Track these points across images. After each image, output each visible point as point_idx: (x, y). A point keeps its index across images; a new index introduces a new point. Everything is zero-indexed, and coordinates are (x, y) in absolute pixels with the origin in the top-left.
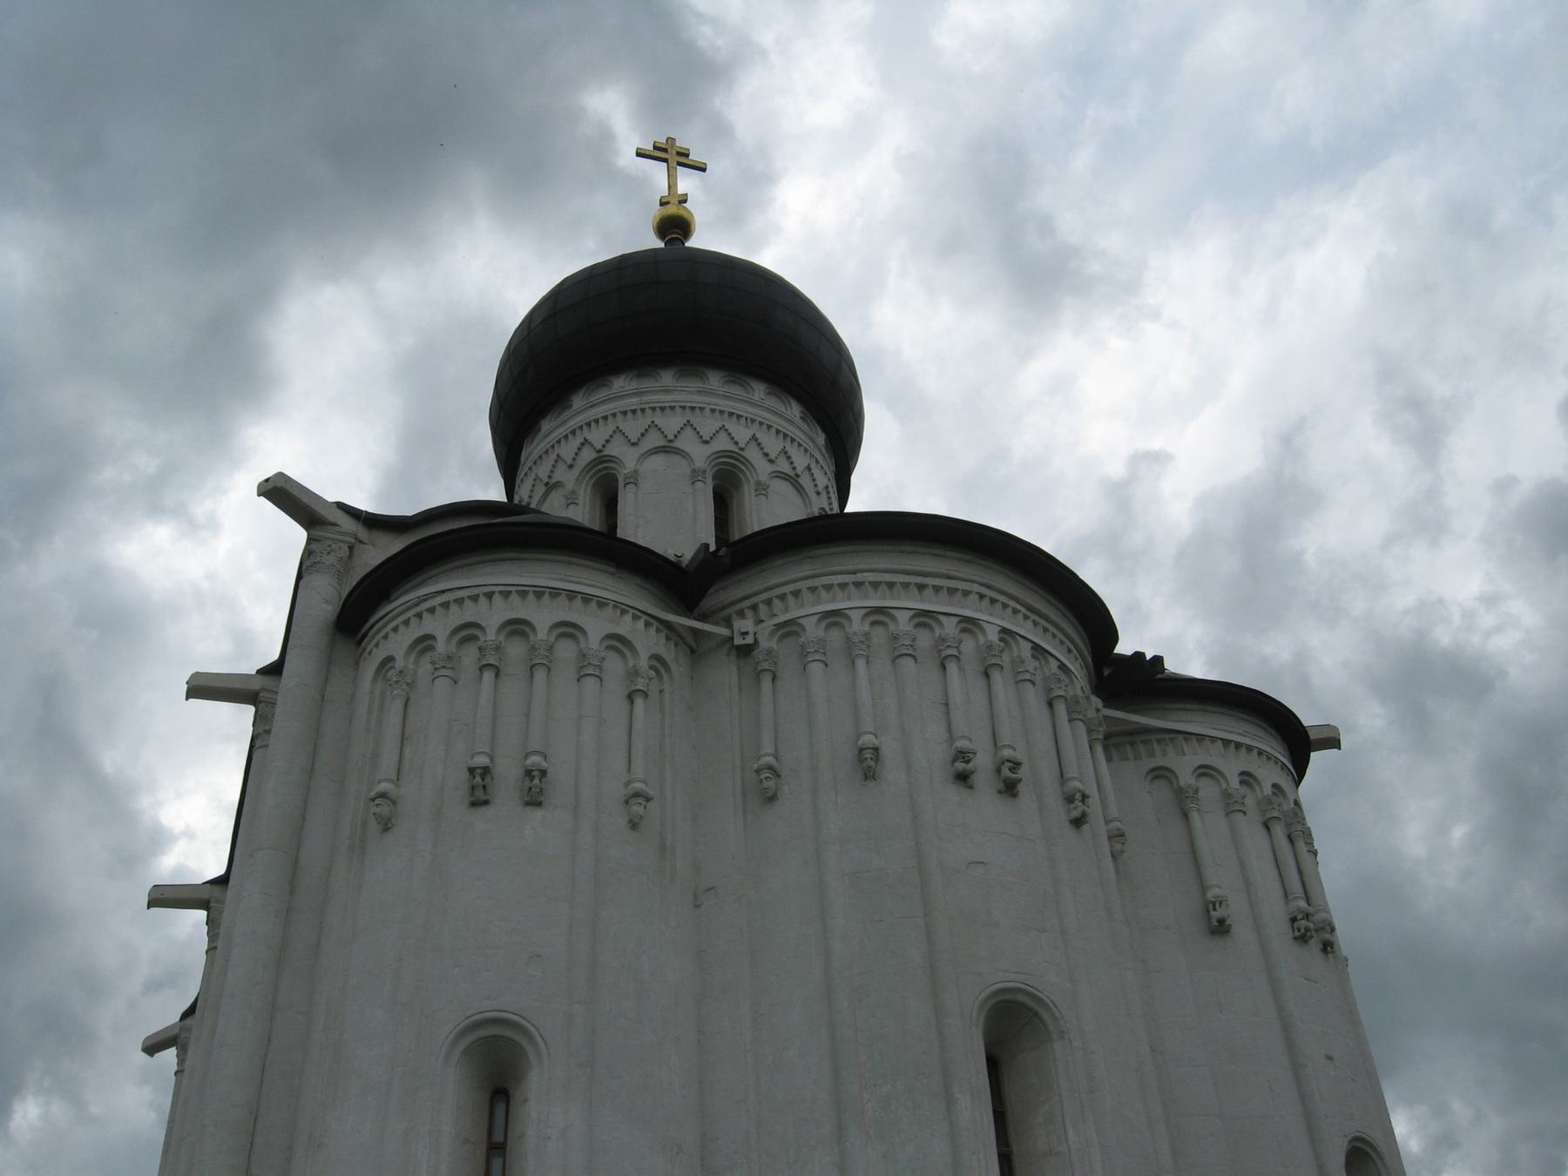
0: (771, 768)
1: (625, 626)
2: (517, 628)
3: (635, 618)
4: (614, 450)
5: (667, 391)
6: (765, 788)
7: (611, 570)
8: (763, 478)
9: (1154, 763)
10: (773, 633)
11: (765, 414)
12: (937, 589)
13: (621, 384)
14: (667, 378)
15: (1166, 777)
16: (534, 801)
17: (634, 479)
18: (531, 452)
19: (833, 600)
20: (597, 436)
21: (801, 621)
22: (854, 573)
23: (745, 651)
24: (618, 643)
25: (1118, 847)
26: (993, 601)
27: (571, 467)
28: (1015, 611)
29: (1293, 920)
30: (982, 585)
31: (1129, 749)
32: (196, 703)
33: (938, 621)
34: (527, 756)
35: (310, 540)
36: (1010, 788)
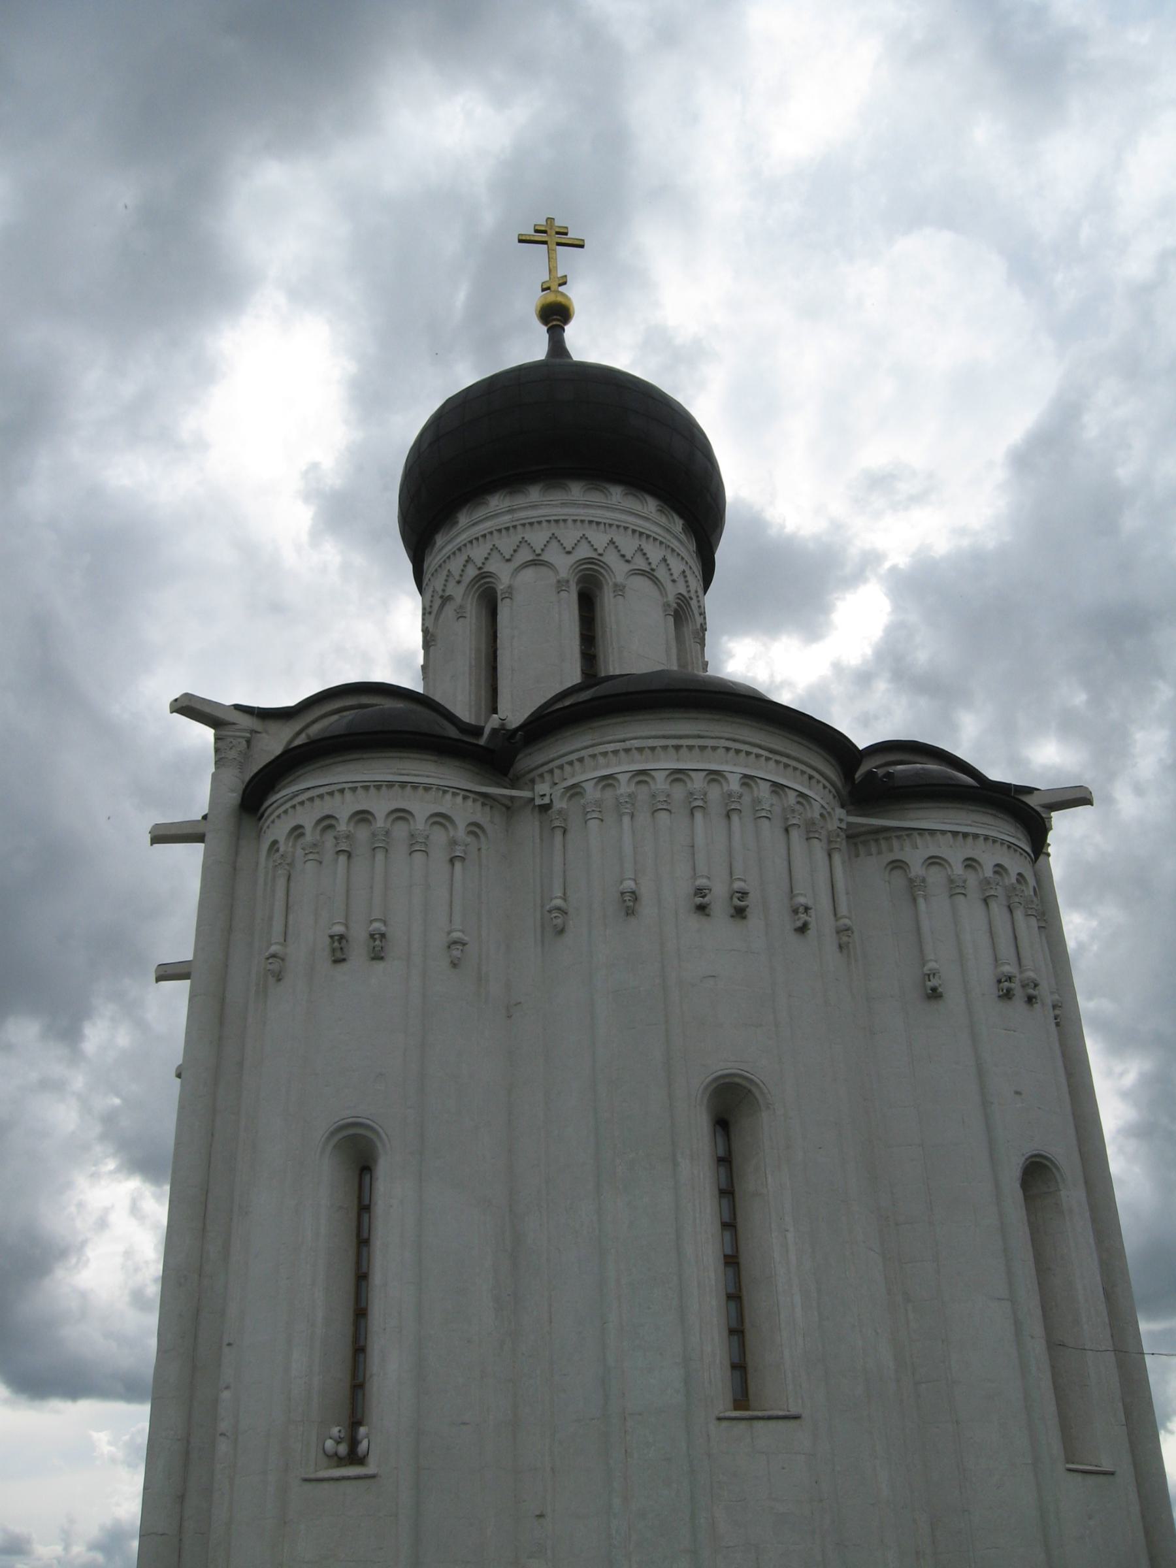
0: (559, 909)
1: (447, 805)
3: (454, 794)
4: (491, 567)
5: (534, 507)
6: (555, 923)
7: (435, 758)
8: (620, 579)
9: (892, 857)
10: (563, 794)
11: (623, 517)
12: (690, 748)
13: (497, 503)
14: (534, 494)
15: (901, 867)
16: (377, 956)
17: (510, 593)
18: (432, 562)
19: (608, 766)
20: (478, 553)
21: (583, 785)
22: (624, 741)
23: (545, 808)
24: (441, 819)
25: (845, 939)
26: (738, 751)
27: (459, 582)
28: (758, 756)
29: (999, 981)
30: (728, 739)
31: (873, 844)
32: (159, 847)
33: (689, 776)
34: (371, 922)
35: (217, 739)
36: (740, 913)
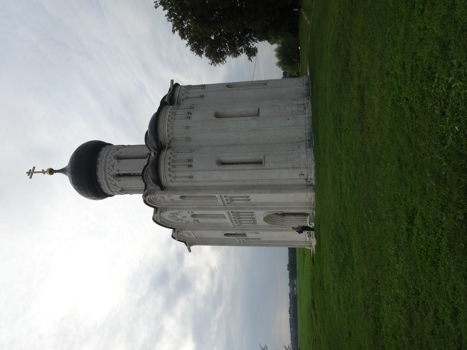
2: (169, 164)
4: (112, 174)
6: (188, 139)
14: (99, 166)
17: (118, 171)
36: (191, 113)
